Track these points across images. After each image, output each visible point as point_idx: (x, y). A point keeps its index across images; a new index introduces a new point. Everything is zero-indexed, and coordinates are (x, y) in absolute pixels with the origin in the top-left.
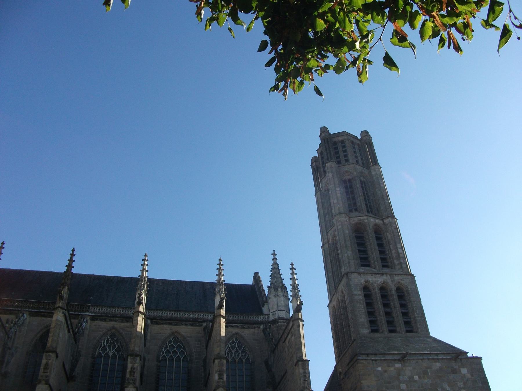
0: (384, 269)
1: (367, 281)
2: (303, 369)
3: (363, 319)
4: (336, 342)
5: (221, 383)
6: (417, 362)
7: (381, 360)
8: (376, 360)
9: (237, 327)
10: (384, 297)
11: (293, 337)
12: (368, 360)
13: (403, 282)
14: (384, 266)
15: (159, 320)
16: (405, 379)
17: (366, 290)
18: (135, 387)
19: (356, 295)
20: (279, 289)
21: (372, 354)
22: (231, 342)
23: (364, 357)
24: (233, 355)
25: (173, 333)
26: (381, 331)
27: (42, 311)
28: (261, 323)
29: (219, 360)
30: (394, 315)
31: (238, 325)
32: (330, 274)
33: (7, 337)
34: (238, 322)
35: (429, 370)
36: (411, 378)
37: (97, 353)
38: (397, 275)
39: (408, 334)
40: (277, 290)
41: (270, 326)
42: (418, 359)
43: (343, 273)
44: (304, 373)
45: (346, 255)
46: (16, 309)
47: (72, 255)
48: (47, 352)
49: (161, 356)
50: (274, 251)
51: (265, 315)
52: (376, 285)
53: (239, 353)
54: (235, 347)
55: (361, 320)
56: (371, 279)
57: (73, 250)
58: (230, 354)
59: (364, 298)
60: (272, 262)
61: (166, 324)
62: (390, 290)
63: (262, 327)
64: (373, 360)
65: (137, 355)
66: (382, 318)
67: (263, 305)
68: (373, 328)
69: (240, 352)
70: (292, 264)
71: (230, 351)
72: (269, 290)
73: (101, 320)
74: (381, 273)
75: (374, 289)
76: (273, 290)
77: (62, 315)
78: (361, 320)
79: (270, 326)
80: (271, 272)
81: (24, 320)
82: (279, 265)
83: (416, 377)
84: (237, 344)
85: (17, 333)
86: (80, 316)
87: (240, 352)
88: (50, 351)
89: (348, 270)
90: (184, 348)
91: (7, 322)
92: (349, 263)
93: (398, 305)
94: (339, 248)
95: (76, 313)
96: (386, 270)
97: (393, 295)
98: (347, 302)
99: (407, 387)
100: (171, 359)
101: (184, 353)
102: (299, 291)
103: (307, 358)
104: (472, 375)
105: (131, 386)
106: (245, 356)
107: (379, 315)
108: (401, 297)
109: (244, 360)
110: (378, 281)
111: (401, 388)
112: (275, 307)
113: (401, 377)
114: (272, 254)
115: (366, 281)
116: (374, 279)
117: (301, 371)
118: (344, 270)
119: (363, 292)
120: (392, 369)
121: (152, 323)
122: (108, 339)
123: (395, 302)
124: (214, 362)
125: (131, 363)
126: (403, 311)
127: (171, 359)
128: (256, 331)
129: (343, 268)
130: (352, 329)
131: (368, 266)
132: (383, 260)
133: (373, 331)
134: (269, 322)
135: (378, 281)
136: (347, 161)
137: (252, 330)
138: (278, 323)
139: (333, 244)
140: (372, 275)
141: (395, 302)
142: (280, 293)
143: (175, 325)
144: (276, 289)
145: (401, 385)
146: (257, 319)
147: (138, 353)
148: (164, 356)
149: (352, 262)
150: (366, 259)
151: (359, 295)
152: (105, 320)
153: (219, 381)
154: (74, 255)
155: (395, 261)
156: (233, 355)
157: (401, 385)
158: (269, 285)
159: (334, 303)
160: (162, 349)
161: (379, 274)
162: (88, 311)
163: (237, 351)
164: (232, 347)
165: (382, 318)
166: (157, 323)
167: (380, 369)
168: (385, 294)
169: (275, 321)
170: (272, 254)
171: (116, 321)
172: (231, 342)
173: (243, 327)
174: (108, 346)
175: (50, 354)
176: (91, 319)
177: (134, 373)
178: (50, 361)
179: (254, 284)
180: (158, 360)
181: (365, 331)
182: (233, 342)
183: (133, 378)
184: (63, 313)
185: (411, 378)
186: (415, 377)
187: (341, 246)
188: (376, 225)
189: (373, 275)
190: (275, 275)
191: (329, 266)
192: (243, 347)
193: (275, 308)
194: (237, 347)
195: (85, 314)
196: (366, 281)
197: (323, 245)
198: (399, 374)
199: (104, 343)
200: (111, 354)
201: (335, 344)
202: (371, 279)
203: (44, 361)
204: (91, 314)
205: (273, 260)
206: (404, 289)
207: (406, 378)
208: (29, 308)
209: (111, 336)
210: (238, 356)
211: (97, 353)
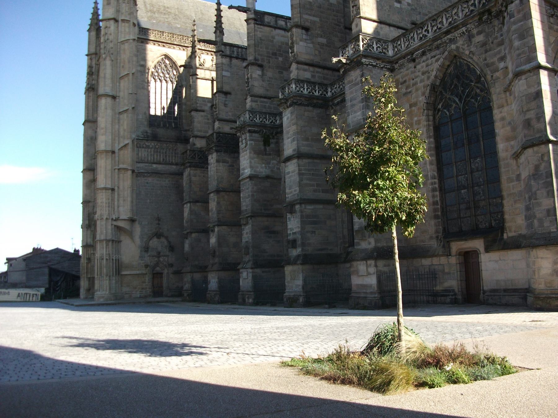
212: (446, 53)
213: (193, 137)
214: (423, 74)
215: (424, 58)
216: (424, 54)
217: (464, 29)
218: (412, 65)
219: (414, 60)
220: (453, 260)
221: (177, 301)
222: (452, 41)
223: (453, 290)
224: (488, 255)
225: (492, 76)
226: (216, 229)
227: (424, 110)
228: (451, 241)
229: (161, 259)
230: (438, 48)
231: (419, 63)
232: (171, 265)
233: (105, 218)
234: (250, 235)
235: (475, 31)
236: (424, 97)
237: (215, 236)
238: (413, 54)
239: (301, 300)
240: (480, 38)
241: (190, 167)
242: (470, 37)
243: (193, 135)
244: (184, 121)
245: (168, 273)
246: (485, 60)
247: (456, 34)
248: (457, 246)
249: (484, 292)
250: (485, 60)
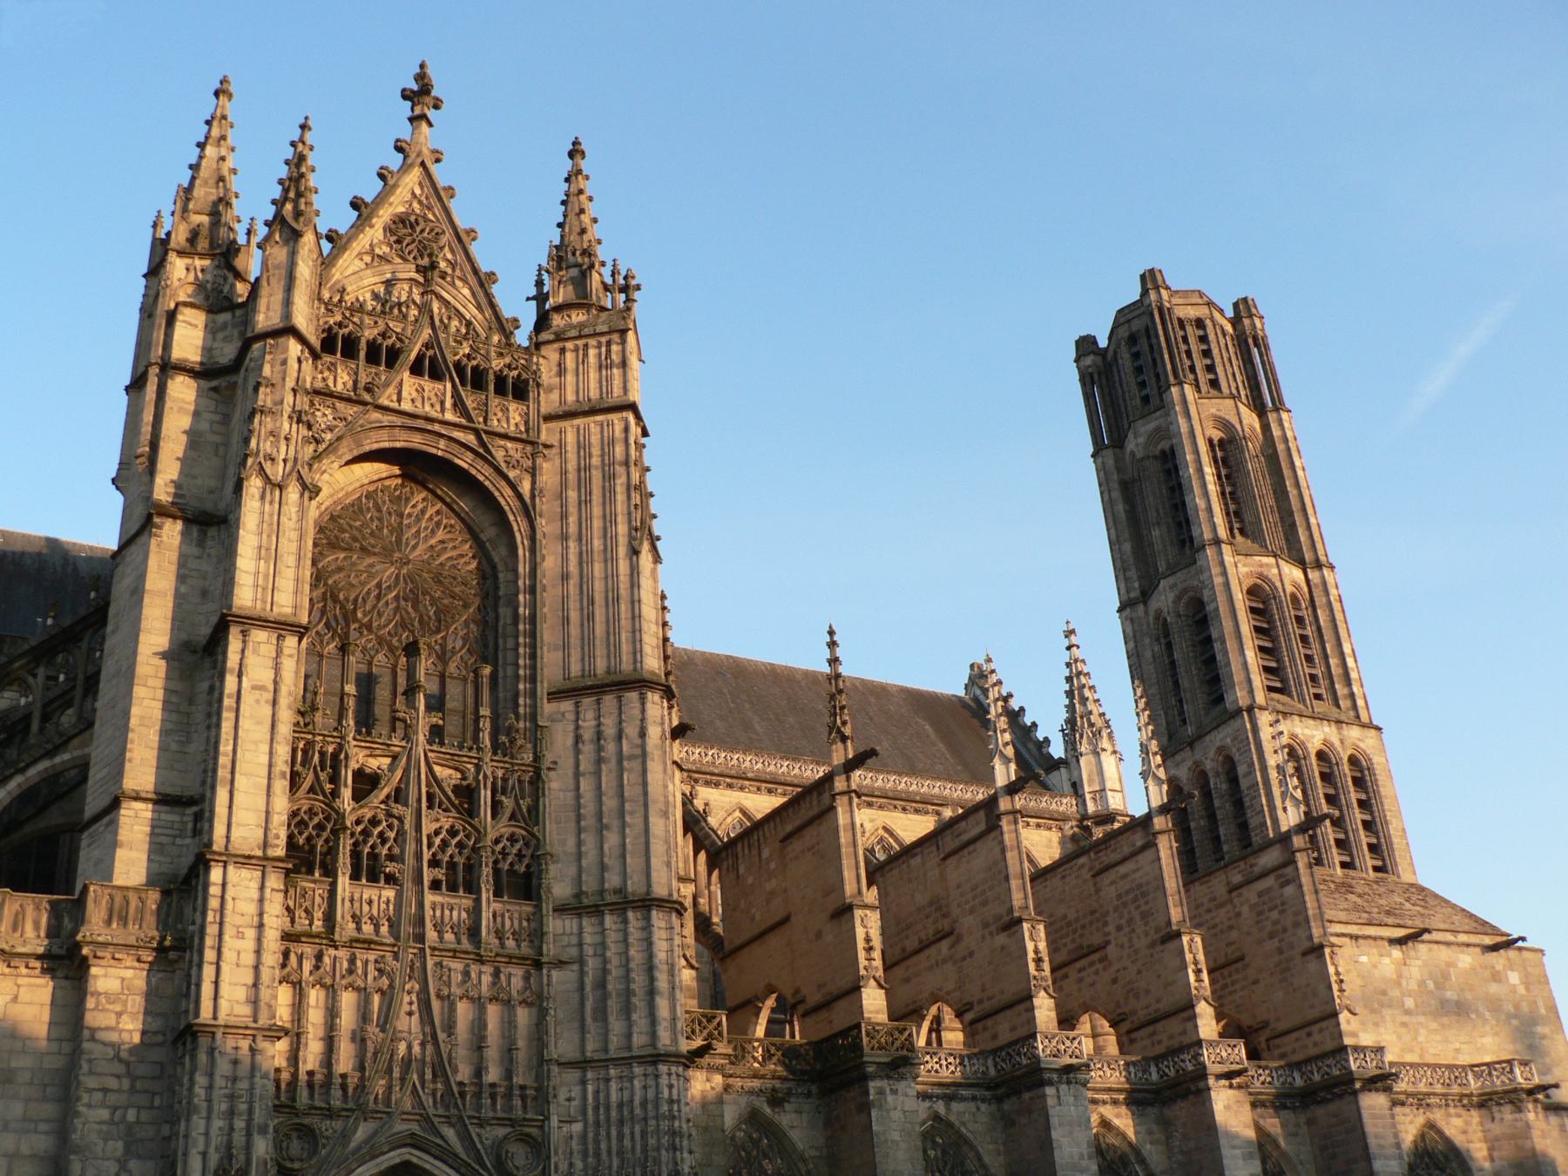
35: (1452, 970)
47: (832, 645)
57: (831, 633)
73: (707, 783)
104: (1528, 989)
108: (1359, 782)
116: (1307, 732)
120: (1386, 960)
136: (1214, 384)
137: (1046, 833)
146: (1054, 806)
152: (717, 785)
155: (1337, 686)
167: (1364, 959)
171: (742, 789)
188: (1296, 585)
191: (1149, 669)
196: (1293, 736)
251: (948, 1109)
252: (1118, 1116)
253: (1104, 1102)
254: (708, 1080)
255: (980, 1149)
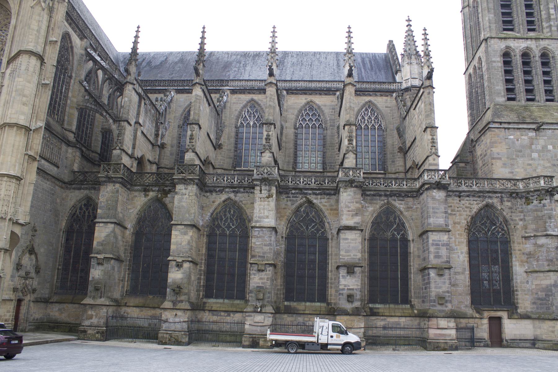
0: (529, 33)
1: (509, 47)
2: (431, 135)
3: (501, 87)
4: (470, 110)
5: (350, 148)
6: (553, 132)
7: (514, 128)
8: (509, 129)
9: (370, 95)
10: (525, 64)
11: (423, 104)
12: (500, 128)
13: (549, 47)
14: (529, 30)
15: (295, 90)
16: (538, 148)
17: (507, 55)
18: (271, 152)
19: (495, 62)
20: (413, 57)
21: (505, 123)
22: (364, 110)
23: (497, 125)
24: (366, 121)
25: (308, 103)
26: (518, 99)
27: (186, 88)
28: (393, 91)
29: (349, 127)
30: (535, 83)
31: (371, 93)
32: (469, 40)
33: (158, 113)
34: (371, 90)
36: (544, 148)
37: (239, 123)
38: (544, 40)
39: (548, 103)
40: (411, 58)
41: (403, 93)
42: (555, 129)
43: (482, 39)
44: (433, 139)
45: (487, 19)
46: (164, 88)
47: (203, 32)
48: (191, 124)
49: (298, 124)
50: (408, 16)
51: (398, 83)
52: (517, 51)
53: (372, 120)
54: (367, 114)
55: (497, 88)
56: (513, 44)
57: (204, 28)
58: (363, 121)
59: (503, 65)
60: (407, 29)
61: (301, 94)
62: (533, 57)
63: (394, 95)
64: (505, 128)
65: (271, 124)
66: (520, 86)
67: (396, 73)
68: (510, 96)
69: (373, 118)
70: (425, 30)
71: (363, 118)
72: (402, 58)
73: (240, 93)
74: (526, 37)
75: (515, 56)
76: (406, 58)
77: (200, 90)
78: (497, 88)
79: (403, 93)
80: (405, 39)
81: (172, 98)
82: (413, 31)
83: (550, 147)
84: (369, 111)
85: (168, 109)
86: (221, 91)
87: (373, 118)
88: (193, 124)
89: (488, 35)
90: (319, 116)
91: (157, 101)
92: (490, 27)
93: (540, 72)
94: (480, 10)
95: (218, 88)
96: (532, 34)
97: (536, 61)
98: (484, 69)
99: (539, 157)
100: (307, 127)
101: (319, 121)
102: (431, 57)
103: (436, 125)
105: (267, 151)
106: (378, 123)
107: (518, 82)
109: (376, 127)
110: (521, 46)
111: (533, 157)
112: (409, 74)
113: (533, 147)
114: (407, 20)
115: (508, 47)
116: (516, 45)
117: (430, 137)
118: (484, 35)
119: (502, 58)
121: (287, 93)
122: (248, 109)
123: (537, 69)
124: (344, 129)
125: (266, 131)
126: (545, 78)
127: (307, 127)
128: (389, 98)
129: (483, 33)
130: (487, 97)
131: (512, 30)
132: (530, 23)
133: (509, 99)
134: (402, 90)
135: (521, 46)
137: (385, 98)
138: (411, 91)
139: (474, 7)
140: (514, 41)
141: (537, 69)
142: (414, 61)
143: (311, 94)
144: (410, 56)
145: (533, 154)
147: (272, 122)
148: (301, 123)
149: (493, 26)
150: (510, 22)
151: (498, 62)
152: (244, 93)
153: (349, 145)
154: (205, 32)
156: (366, 121)
157: (533, 154)
158: (403, 53)
159: (471, 70)
160: (298, 117)
161: (522, 38)
162: (228, 86)
163: (370, 118)
164: (365, 114)
165: (520, 86)
166: (293, 93)
167: (512, 137)
168: (527, 60)
169: (407, 89)
170: (407, 20)
171: (254, 94)
172: (364, 110)
173: (376, 95)
174: (249, 116)
175: (194, 126)
176: (231, 93)
177: (270, 139)
178: (194, 132)
179: (388, 52)
180: (296, 128)
181: (501, 99)
182: (366, 110)
183: (269, 144)
184: (201, 88)
185: (544, 148)
186: (549, 146)
187: (482, 9)
189: (516, 40)
190: (409, 42)
191: (468, 32)
192: (376, 114)
193: (408, 76)
194: (369, 114)
195: (225, 88)
196: (508, 47)
197: (463, 8)
198: (532, 144)
199: (245, 114)
200: (252, 124)
201: (469, 112)
202: (513, 44)
203: (189, 133)
204: (230, 88)
205: (407, 26)
206: (551, 55)
207: (539, 147)
208: (175, 86)
209: (250, 107)
210: (371, 122)
211: (239, 123)
212: (484, 203)
213: (120, 149)
214: (466, 207)
215: (468, 198)
216: (468, 196)
217: (499, 195)
218: (458, 199)
219: (460, 197)
220: (486, 321)
221: (69, 340)
222: (490, 197)
223: (484, 339)
224: (509, 320)
225: (515, 226)
226: (186, 265)
227: (466, 229)
228: (485, 310)
229: (27, 282)
230: (479, 197)
231: (463, 200)
232: (34, 291)
233: (8, 219)
234: (269, 282)
235: (505, 199)
236: (466, 221)
237: (182, 270)
238: (460, 193)
239: (363, 344)
240: (509, 204)
241: (120, 183)
242: (502, 202)
243: (122, 148)
244: (66, 118)
245: (29, 301)
246: (511, 216)
247: (495, 195)
248: (486, 314)
249: (506, 340)
250: (511, 216)
251: (236, 196)
252: (317, 199)
253: (310, 194)
254: (114, 186)
255: (247, 211)
